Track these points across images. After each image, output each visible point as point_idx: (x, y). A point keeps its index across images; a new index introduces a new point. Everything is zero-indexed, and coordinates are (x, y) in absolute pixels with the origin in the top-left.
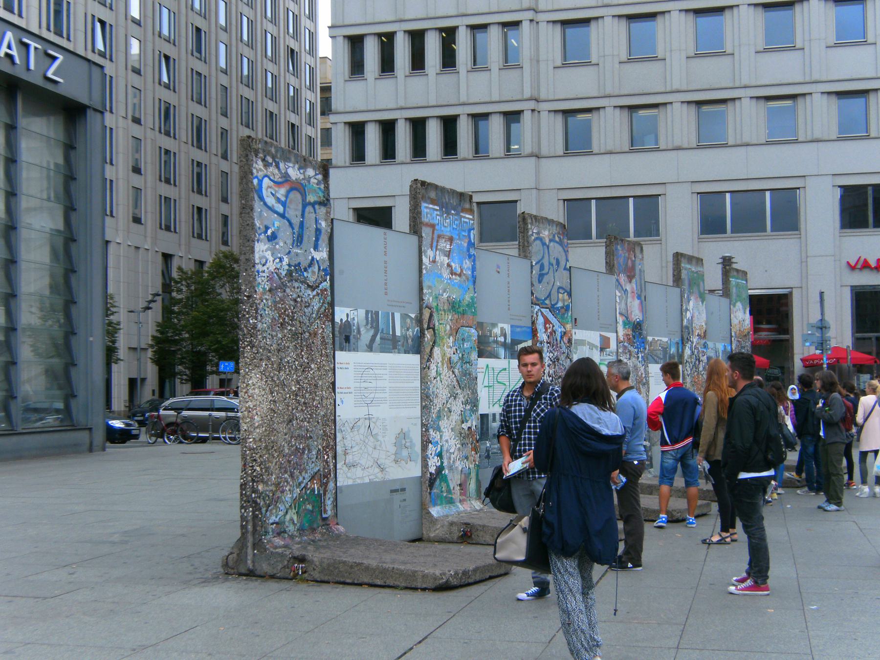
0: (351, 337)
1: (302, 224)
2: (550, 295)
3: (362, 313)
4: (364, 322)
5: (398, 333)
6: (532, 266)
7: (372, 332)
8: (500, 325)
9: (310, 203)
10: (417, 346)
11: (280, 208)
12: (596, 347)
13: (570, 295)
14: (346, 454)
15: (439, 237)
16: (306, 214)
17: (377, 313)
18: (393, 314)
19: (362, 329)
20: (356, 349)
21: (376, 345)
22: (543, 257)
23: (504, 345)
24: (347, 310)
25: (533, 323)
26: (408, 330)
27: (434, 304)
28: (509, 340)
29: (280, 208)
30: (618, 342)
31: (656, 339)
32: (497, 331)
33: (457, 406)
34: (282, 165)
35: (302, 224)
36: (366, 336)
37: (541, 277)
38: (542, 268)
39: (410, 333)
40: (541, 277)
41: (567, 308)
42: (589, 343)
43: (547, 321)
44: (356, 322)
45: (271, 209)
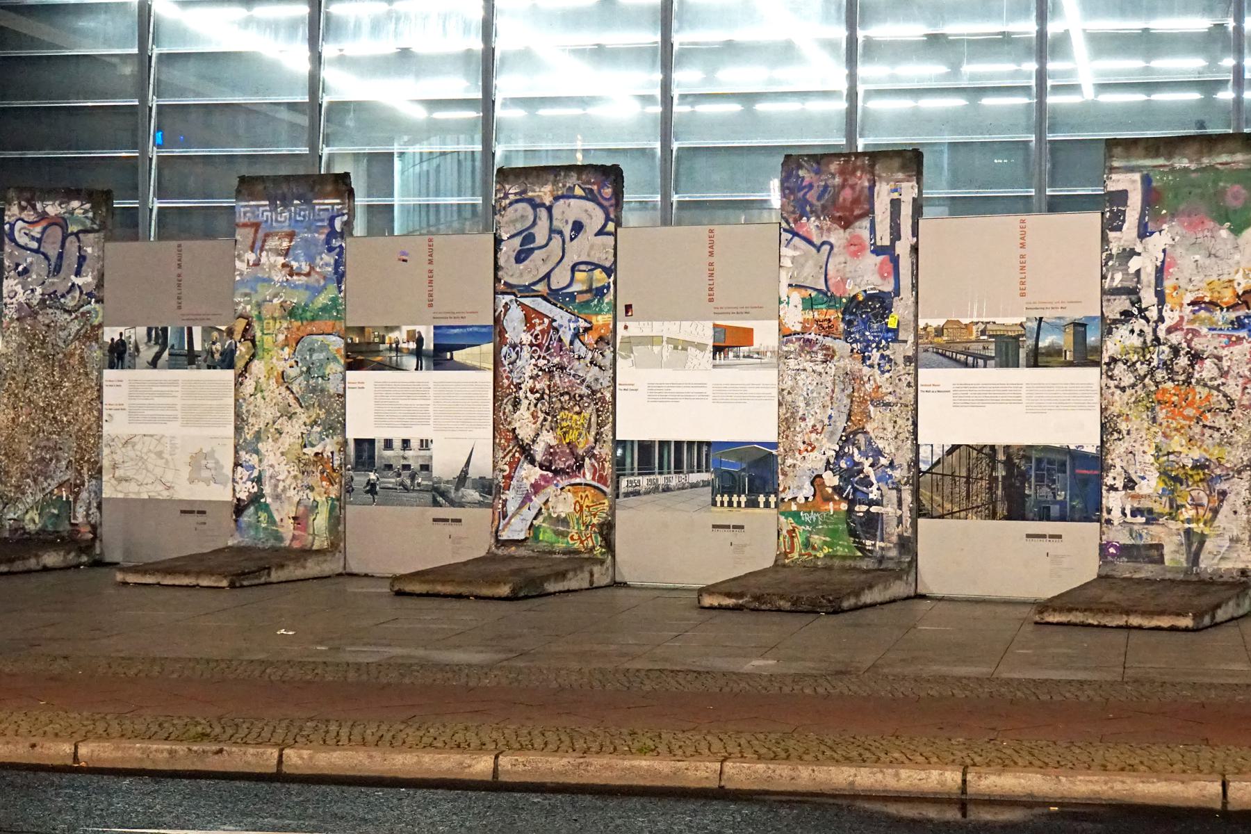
0: (127, 355)
3: (142, 331)
4: (146, 339)
5: (198, 346)
6: (498, 241)
7: (157, 349)
8: (405, 329)
9: (72, 234)
10: (227, 360)
11: (35, 245)
12: (701, 347)
14: (115, 467)
15: (267, 235)
16: (67, 244)
17: (165, 330)
18: (190, 330)
19: (142, 348)
20: (132, 366)
21: (160, 362)
22: (534, 223)
23: (419, 353)
24: (122, 329)
25: (497, 320)
26: (214, 343)
27: (254, 313)
28: (429, 345)
29: (35, 245)
30: (786, 335)
32: (401, 335)
33: (294, 429)
34: (39, 206)
35: (60, 256)
36: (148, 353)
37: (521, 257)
38: (529, 238)
39: (218, 346)
40: (521, 257)
41: (600, 292)
42: (670, 341)
43: (530, 316)
44: (132, 340)
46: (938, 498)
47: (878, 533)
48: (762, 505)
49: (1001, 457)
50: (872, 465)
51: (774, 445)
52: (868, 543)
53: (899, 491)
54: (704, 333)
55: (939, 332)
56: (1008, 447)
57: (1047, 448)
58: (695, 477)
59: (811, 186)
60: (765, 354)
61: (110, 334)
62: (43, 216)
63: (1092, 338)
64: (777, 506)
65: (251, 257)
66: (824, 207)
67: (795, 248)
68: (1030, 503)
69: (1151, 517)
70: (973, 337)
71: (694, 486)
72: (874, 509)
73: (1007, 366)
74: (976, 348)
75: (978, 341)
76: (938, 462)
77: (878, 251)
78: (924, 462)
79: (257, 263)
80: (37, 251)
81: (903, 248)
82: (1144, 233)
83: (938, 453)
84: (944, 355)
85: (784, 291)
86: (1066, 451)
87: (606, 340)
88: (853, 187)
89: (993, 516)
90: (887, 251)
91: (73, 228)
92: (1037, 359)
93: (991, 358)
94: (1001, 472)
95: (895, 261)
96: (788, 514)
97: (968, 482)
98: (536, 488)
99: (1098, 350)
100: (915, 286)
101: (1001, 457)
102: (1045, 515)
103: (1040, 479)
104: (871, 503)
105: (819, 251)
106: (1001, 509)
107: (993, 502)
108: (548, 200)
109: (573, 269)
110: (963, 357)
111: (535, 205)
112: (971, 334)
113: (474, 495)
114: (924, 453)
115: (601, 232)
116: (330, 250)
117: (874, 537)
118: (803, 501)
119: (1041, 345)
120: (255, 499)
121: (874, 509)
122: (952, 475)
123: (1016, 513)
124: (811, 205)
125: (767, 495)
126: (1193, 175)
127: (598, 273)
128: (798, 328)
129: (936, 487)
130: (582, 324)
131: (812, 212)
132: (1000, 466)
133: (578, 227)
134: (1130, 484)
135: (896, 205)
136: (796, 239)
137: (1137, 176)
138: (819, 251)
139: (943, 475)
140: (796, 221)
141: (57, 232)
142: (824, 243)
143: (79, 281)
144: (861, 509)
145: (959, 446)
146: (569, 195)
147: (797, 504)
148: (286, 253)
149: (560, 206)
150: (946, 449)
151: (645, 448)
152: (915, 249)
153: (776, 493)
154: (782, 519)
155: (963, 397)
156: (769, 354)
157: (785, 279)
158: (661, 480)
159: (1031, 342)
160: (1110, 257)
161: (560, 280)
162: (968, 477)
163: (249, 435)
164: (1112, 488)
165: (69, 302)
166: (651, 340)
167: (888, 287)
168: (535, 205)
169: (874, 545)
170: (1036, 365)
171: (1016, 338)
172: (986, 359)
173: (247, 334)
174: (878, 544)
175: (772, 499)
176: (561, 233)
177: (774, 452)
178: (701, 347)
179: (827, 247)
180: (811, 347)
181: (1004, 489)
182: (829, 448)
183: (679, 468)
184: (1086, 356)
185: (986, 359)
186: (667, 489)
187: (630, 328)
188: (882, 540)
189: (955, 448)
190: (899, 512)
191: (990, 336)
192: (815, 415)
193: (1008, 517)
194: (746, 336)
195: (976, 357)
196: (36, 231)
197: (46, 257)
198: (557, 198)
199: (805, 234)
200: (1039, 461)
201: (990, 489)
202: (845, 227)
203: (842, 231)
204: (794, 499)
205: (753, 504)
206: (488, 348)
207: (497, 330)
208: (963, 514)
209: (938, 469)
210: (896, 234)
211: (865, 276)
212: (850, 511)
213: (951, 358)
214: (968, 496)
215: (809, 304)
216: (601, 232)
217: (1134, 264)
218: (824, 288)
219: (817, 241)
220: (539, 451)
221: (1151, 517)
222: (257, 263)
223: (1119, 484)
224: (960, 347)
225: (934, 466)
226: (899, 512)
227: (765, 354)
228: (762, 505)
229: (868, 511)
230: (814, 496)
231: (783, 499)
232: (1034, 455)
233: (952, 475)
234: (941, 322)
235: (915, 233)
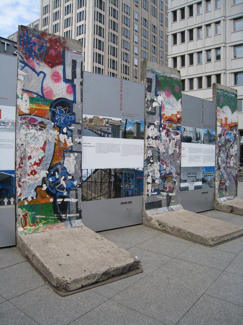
30: (21, 115)
31: (101, 117)
46: (89, 192)
47: (68, 211)
48: (6, 204)
49: (113, 173)
50: (64, 180)
51: (13, 172)
52: (63, 215)
53: (76, 190)
55: (91, 120)
56: (115, 169)
57: (128, 169)
59: (35, 44)
60: (8, 123)
63: (142, 129)
64: (15, 203)
66: (41, 55)
67: (26, 72)
68: (122, 190)
70: (104, 124)
72: (66, 200)
73: (115, 137)
74: (105, 129)
75: (105, 126)
76: (90, 177)
77: (66, 81)
78: (84, 177)
81: (77, 82)
82: (157, 95)
83: (90, 172)
84: (93, 131)
85: (19, 93)
86: (133, 170)
88: (56, 50)
89: (110, 197)
90: (70, 82)
92: (126, 135)
93: (110, 134)
94: (113, 179)
95: (74, 87)
96: (22, 207)
97: (101, 184)
99: (143, 133)
101: (113, 173)
102: (127, 195)
103: (126, 181)
104: (64, 197)
105: (38, 75)
106: (113, 194)
107: (110, 191)
110: (100, 132)
112: (103, 123)
114: (84, 173)
117: (65, 213)
118: (31, 199)
119: (127, 130)
121: (66, 200)
122: (95, 182)
123: (118, 195)
124: (35, 53)
125: (9, 198)
126: (168, 79)
128: (28, 112)
129: (89, 187)
131: (35, 56)
132: (112, 177)
134: (153, 181)
136: (26, 68)
137: (154, 75)
138: (38, 75)
139: (92, 182)
140: (27, 58)
142: (41, 72)
144: (59, 200)
145: (98, 170)
147: (27, 201)
150: (93, 171)
152: (81, 84)
153: (15, 198)
154: (19, 211)
155: (101, 149)
156: (10, 124)
157: (20, 87)
159: (123, 128)
160: (148, 100)
162: (101, 182)
164: (148, 183)
167: (70, 98)
169: (66, 216)
170: (125, 137)
171: (119, 126)
172: (109, 134)
174: (68, 215)
175: (12, 200)
177: (13, 175)
179: (42, 75)
180: (34, 122)
181: (114, 186)
182: (43, 173)
184: (140, 135)
185: (109, 134)
188: (70, 213)
189: (96, 170)
190: (76, 200)
191: (110, 125)
192: (37, 155)
193: (115, 197)
195: (105, 133)
199: (31, 66)
200: (125, 174)
201: (109, 186)
202: (52, 67)
203: (50, 68)
204: (26, 199)
208: (99, 198)
209: (90, 180)
210: (74, 75)
211: (60, 90)
212: (55, 201)
213: (98, 134)
214: (101, 191)
215: (32, 100)
217: (155, 104)
219: (38, 70)
223: (151, 182)
224: (98, 128)
225: (88, 178)
226: (76, 200)
227: (8, 123)
228: (6, 204)
229: (63, 201)
230: (36, 196)
231: (20, 200)
232: (124, 172)
233: (95, 182)
234: (92, 117)
235: (82, 77)
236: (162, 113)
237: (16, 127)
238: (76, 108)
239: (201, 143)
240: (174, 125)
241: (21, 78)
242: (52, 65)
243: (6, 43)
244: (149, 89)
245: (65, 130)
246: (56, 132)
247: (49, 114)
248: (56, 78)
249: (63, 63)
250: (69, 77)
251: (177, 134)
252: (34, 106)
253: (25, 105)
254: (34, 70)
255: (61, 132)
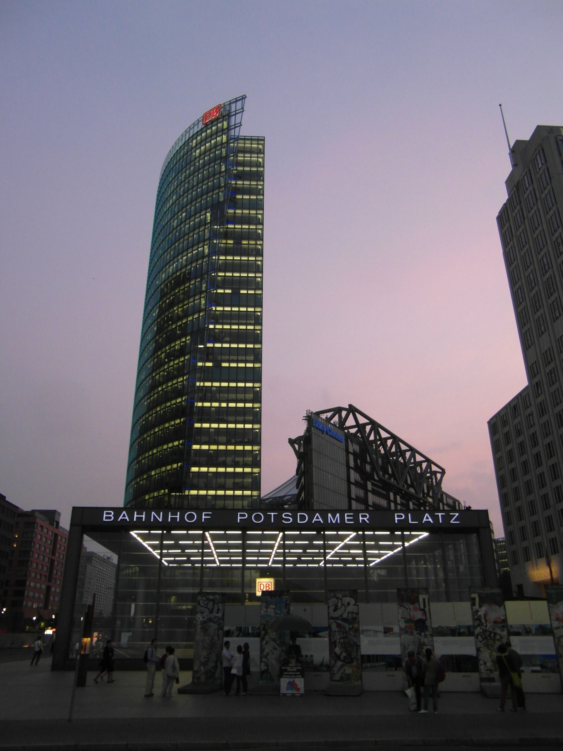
1: (213, 609)
2: (342, 615)
3: (234, 628)
5: (250, 631)
6: (329, 607)
10: (258, 635)
12: (381, 632)
13: (357, 614)
17: (241, 628)
19: (235, 632)
20: (232, 637)
30: (401, 629)
35: (213, 609)
37: (335, 610)
40: (335, 610)
41: (356, 618)
45: (203, 607)
54: (381, 628)
55: (437, 628)
58: (381, 664)
61: (226, 628)
62: (208, 599)
63: (472, 630)
65: (265, 610)
69: (491, 671)
71: (382, 665)
77: (421, 610)
79: (267, 611)
80: (206, 607)
81: (427, 609)
85: (400, 619)
87: (357, 631)
90: (423, 610)
91: (216, 602)
95: (425, 612)
98: (342, 666)
100: (430, 618)
108: (341, 597)
109: (348, 613)
111: (338, 598)
113: (325, 669)
115: (354, 605)
116: (286, 608)
120: (266, 671)
127: (354, 615)
130: (351, 626)
133: (349, 604)
135: (424, 599)
141: (211, 603)
143: (218, 615)
146: (346, 596)
148: (274, 609)
149: (344, 599)
151: (369, 656)
158: (373, 664)
161: (345, 616)
163: (265, 654)
165: (215, 620)
166: (368, 630)
167: (424, 618)
168: (338, 598)
173: (264, 629)
176: (344, 605)
178: (381, 632)
183: (377, 662)
186: (375, 667)
187: (363, 627)
194: (392, 629)
196: (206, 602)
197: (208, 609)
198: (343, 597)
205: (396, 670)
206: (327, 632)
207: (329, 628)
211: (418, 615)
215: (406, 622)
216: (354, 605)
217: (479, 613)
218: (408, 617)
220: (342, 658)
221: (491, 671)
222: (267, 611)
236: (487, 618)
237: (400, 635)
238: (428, 623)
239: (533, 635)
240: (499, 625)
241: (400, 612)
242: (413, 603)
243: (440, 514)
244: (473, 604)
245: (423, 634)
246: (417, 636)
247: (414, 627)
248: (416, 609)
249: (418, 601)
250: (422, 607)
251: (503, 631)
252: (408, 624)
253: (403, 625)
254: (405, 607)
255: (421, 635)
